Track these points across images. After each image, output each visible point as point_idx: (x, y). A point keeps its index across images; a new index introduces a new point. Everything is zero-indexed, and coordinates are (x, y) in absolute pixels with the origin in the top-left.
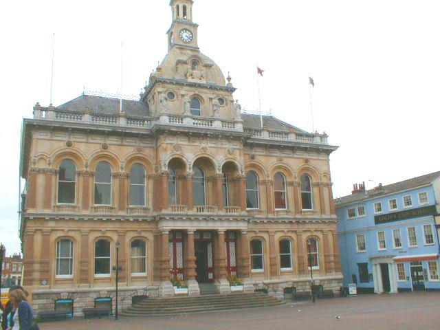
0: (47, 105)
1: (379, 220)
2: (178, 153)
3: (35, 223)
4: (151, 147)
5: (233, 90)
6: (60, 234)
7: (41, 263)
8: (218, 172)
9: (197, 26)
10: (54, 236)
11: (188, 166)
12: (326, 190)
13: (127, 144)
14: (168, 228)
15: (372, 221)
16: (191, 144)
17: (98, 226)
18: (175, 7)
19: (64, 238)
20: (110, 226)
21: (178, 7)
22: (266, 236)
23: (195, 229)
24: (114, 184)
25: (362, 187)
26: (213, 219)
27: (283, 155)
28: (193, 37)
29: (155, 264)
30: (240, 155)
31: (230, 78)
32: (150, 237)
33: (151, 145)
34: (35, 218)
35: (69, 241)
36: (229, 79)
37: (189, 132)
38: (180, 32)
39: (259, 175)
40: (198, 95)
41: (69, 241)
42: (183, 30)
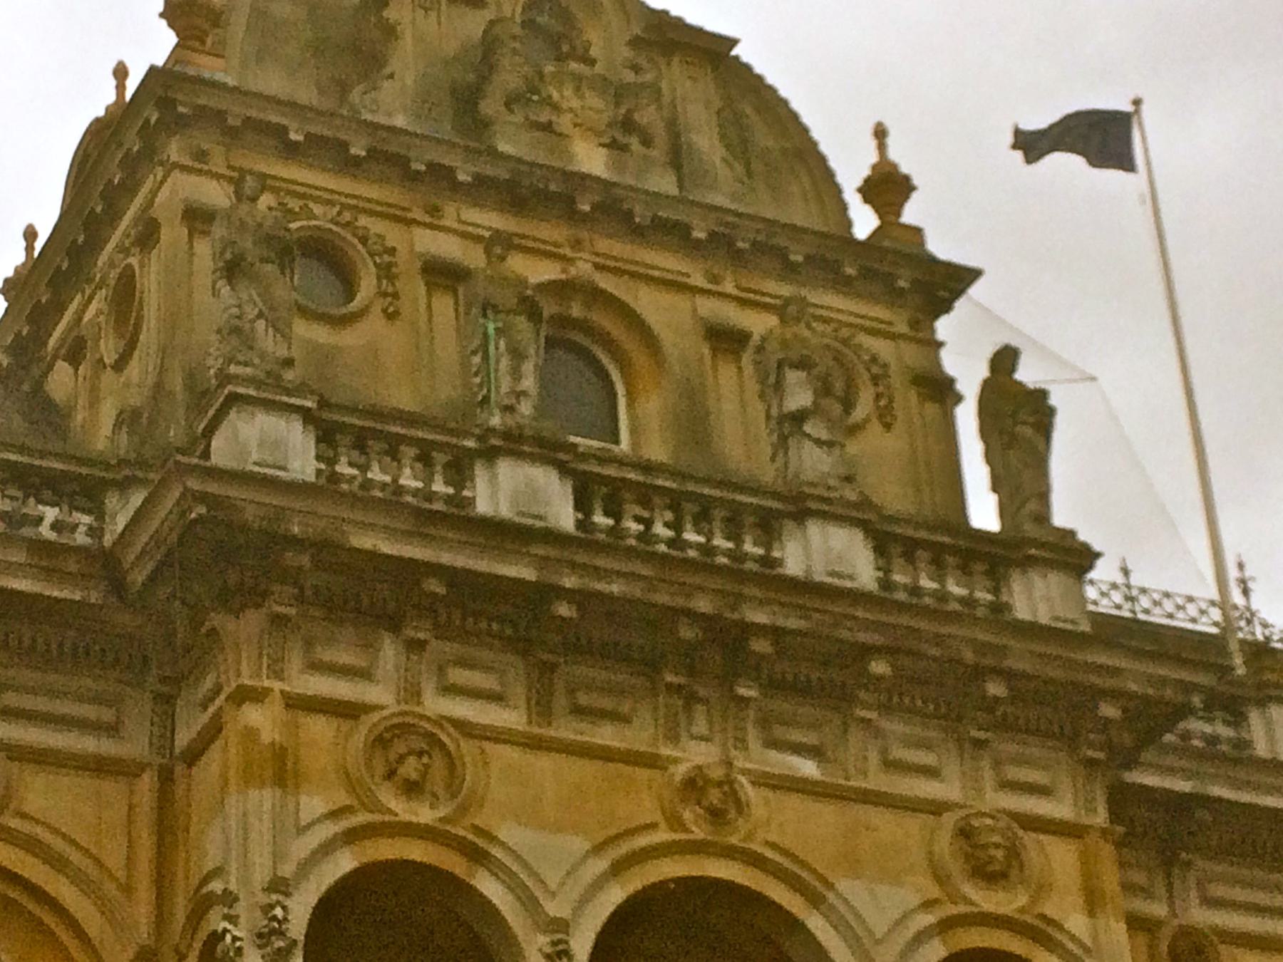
2: (425, 815)
4: (99, 767)
30: (1093, 902)
33: (89, 744)
37: (546, 592)
40: (597, 296)
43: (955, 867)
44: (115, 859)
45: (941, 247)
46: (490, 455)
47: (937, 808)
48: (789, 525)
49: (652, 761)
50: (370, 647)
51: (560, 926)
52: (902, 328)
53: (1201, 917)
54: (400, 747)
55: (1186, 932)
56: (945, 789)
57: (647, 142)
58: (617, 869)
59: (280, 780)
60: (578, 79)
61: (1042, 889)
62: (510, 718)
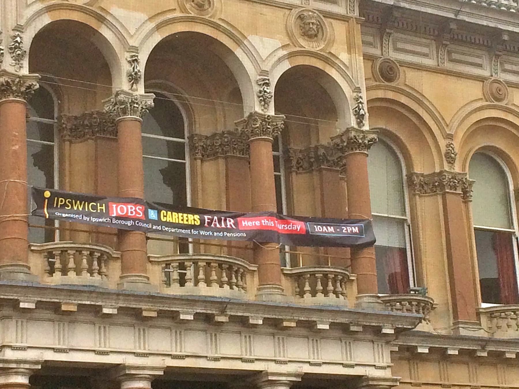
8: (258, 109)
11: (126, 68)
14: (31, 355)
26: (243, 322)
27: (504, 77)
30: (350, 48)
39: (413, 149)
43: (297, 32)
51: (136, 49)
53: (394, 56)
55: (387, 61)
58: (158, 27)
61: (331, 42)
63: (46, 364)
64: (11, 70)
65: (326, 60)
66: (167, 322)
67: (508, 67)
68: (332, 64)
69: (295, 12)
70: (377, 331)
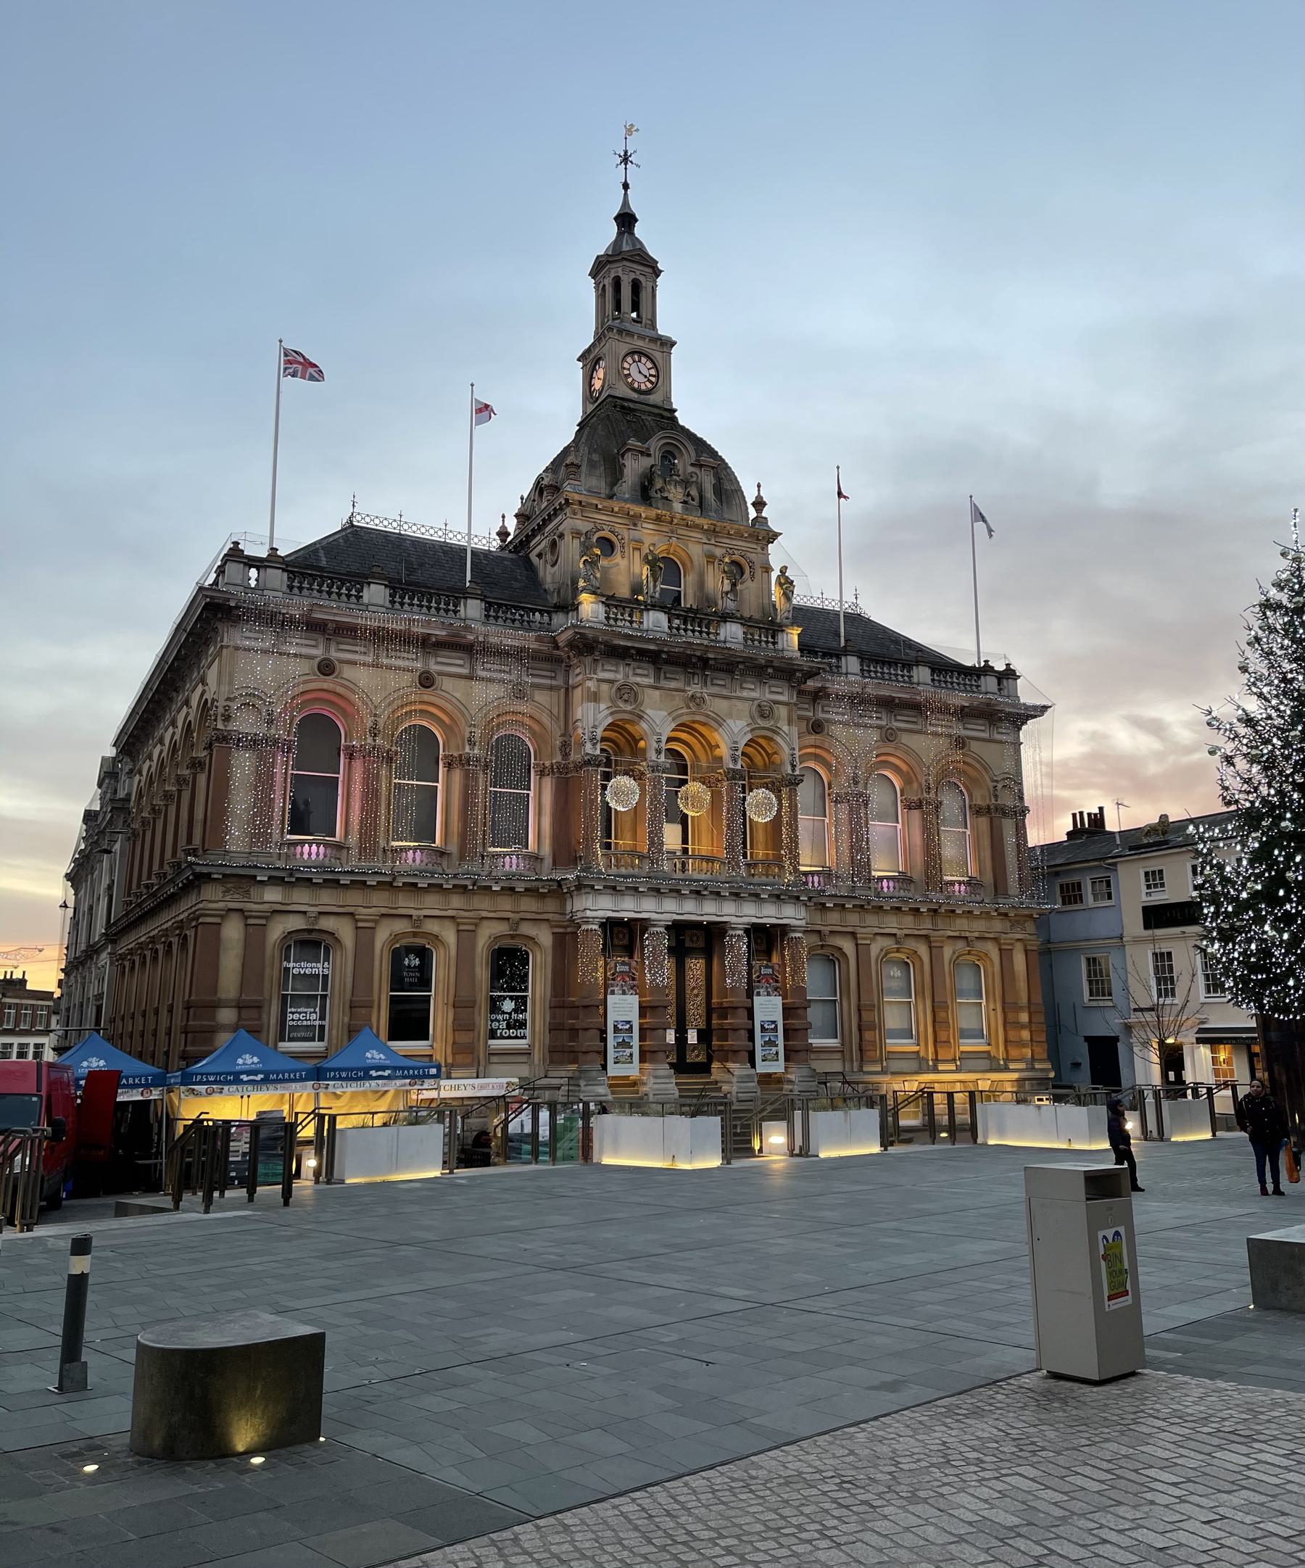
0: (263, 553)
1: (1157, 916)
2: (629, 708)
3: (227, 891)
4: (551, 688)
5: (773, 537)
6: (296, 923)
7: (240, 1006)
9: (673, 344)
10: (277, 930)
12: (1008, 826)
13: (488, 675)
15: (1133, 924)
16: (663, 683)
17: (405, 903)
18: (608, 282)
19: (306, 936)
20: (432, 904)
21: (617, 283)
22: (848, 946)
23: (669, 918)
24: (445, 786)
25: (1098, 820)
28: (661, 374)
29: (553, 1016)
30: (790, 723)
31: (765, 504)
32: (545, 937)
33: (548, 682)
34: (225, 876)
35: (317, 944)
36: (759, 504)
38: (624, 359)
41: (317, 944)
42: (632, 353)
43: (756, 715)
44: (555, 711)
45: (774, 525)
46: (648, 610)
47: (753, 700)
48: (722, 624)
49: (684, 691)
50: (616, 665)
52: (759, 550)
54: (623, 692)
56: (753, 695)
57: (693, 500)
59: (595, 701)
60: (676, 482)
61: (777, 720)
62: (650, 681)
63: (608, 918)
64: (590, 752)
65: (774, 732)
66: (674, 894)
67: (899, 718)
68: (778, 734)
69: (756, 703)
70: (798, 898)
